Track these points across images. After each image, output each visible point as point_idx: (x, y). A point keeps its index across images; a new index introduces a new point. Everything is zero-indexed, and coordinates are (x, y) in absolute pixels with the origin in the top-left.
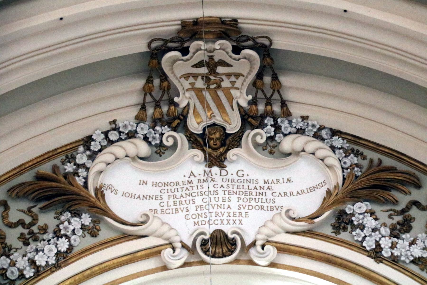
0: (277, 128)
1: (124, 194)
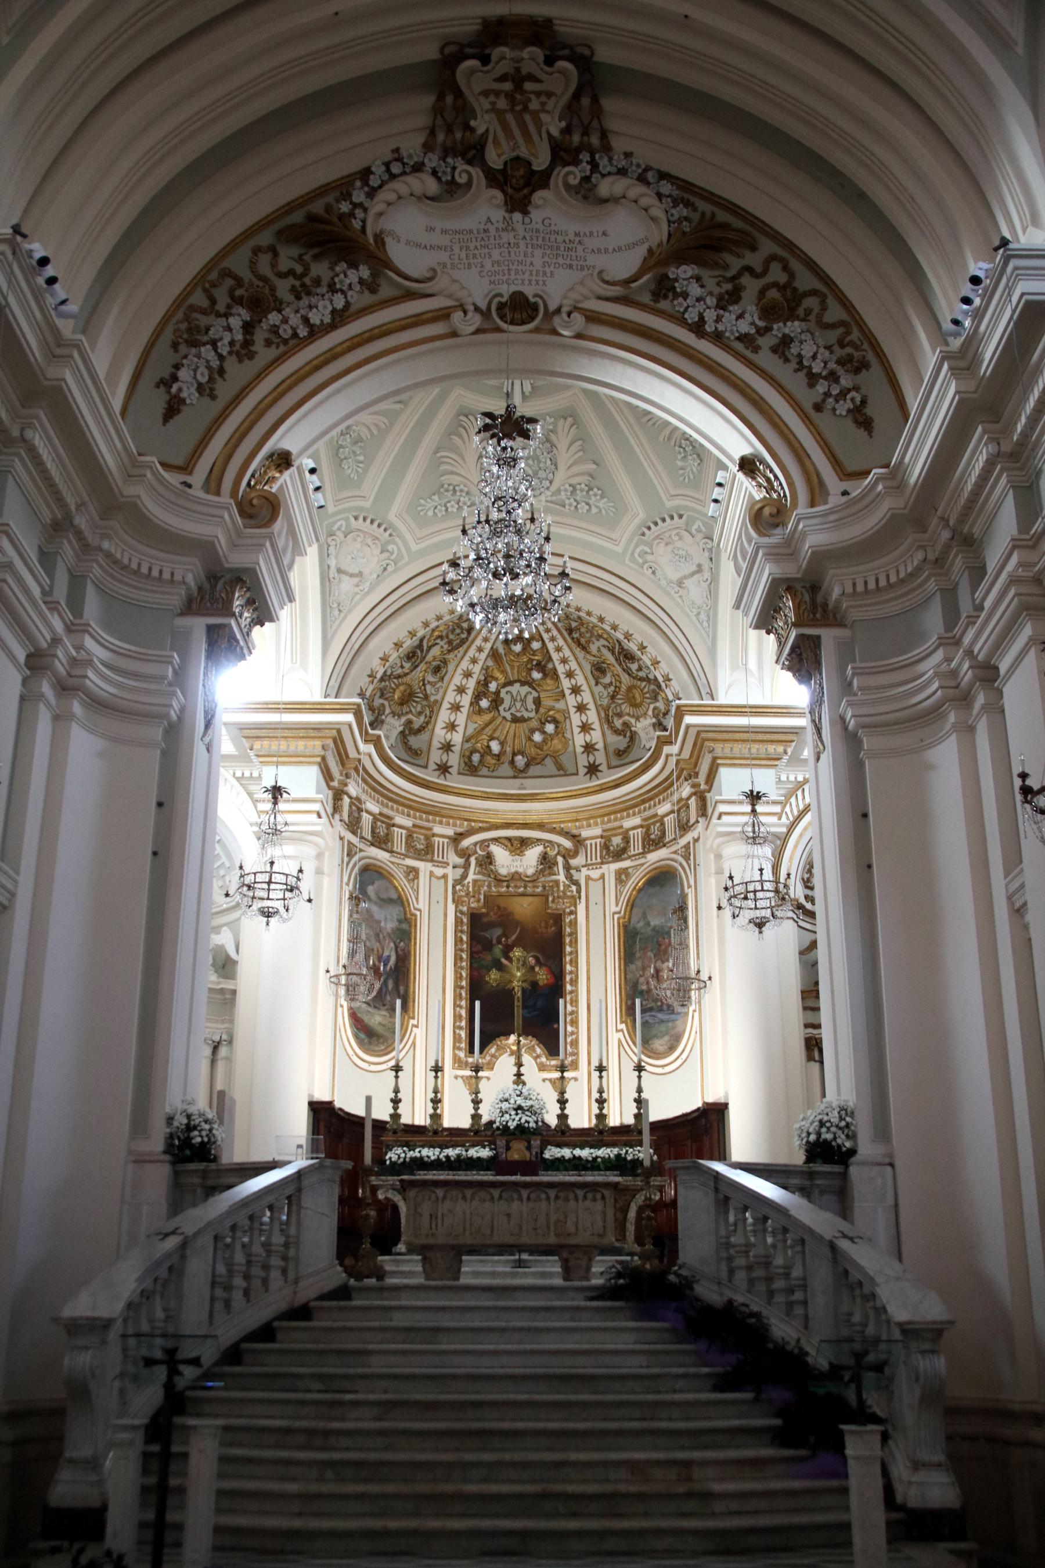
0: (594, 166)
1: (408, 243)
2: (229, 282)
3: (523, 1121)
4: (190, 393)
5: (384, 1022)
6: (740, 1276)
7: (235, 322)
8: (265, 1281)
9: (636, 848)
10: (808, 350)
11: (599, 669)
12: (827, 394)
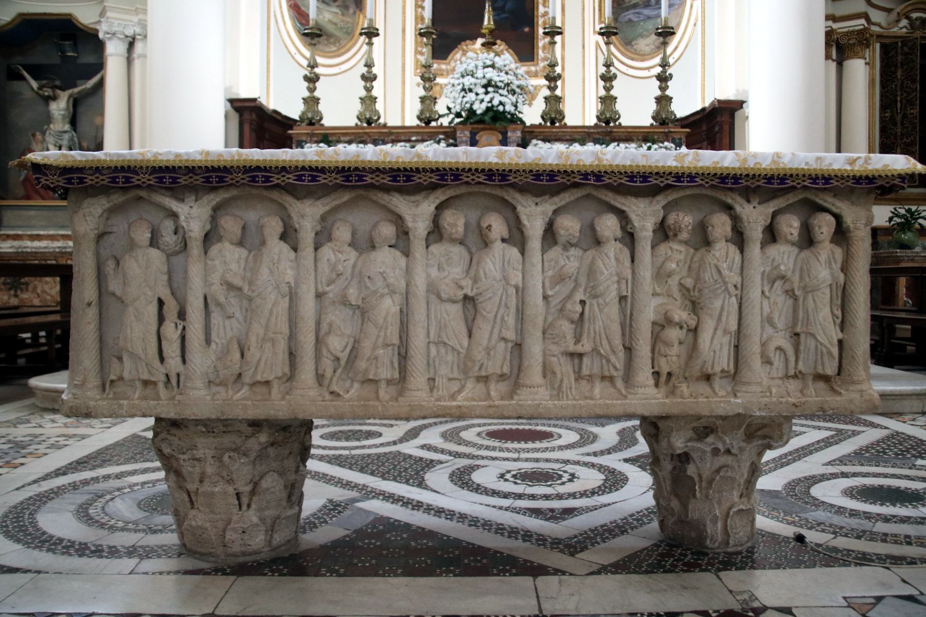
3: (495, 102)
5: (335, 20)
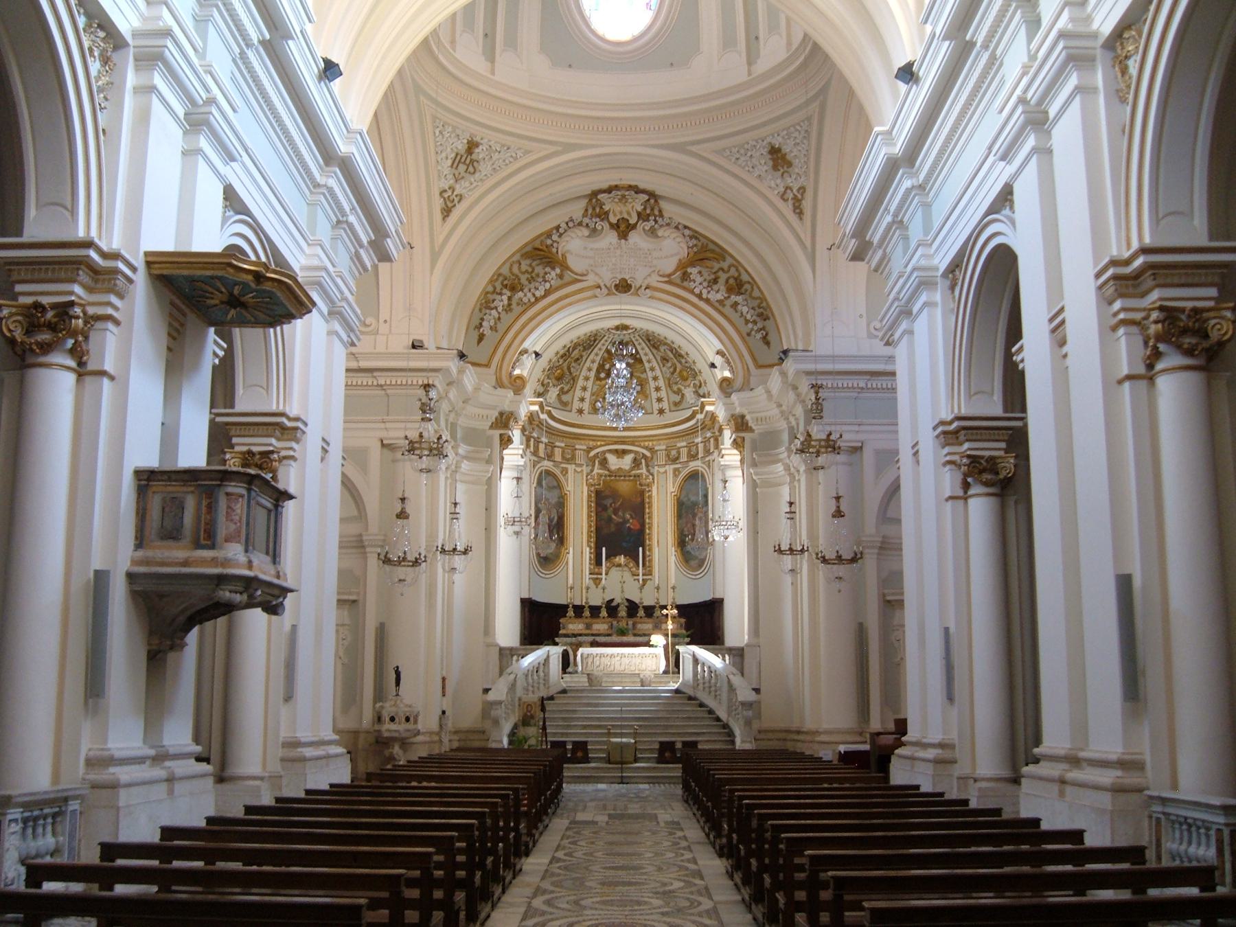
0: (656, 222)
2: (501, 279)
4: (487, 332)
6: (701, 685)
7: (505, 298)
8: (538, 688)
9: (684, 458)
10: (745, 309)
11: (665, 360)
12: (752, 329)
